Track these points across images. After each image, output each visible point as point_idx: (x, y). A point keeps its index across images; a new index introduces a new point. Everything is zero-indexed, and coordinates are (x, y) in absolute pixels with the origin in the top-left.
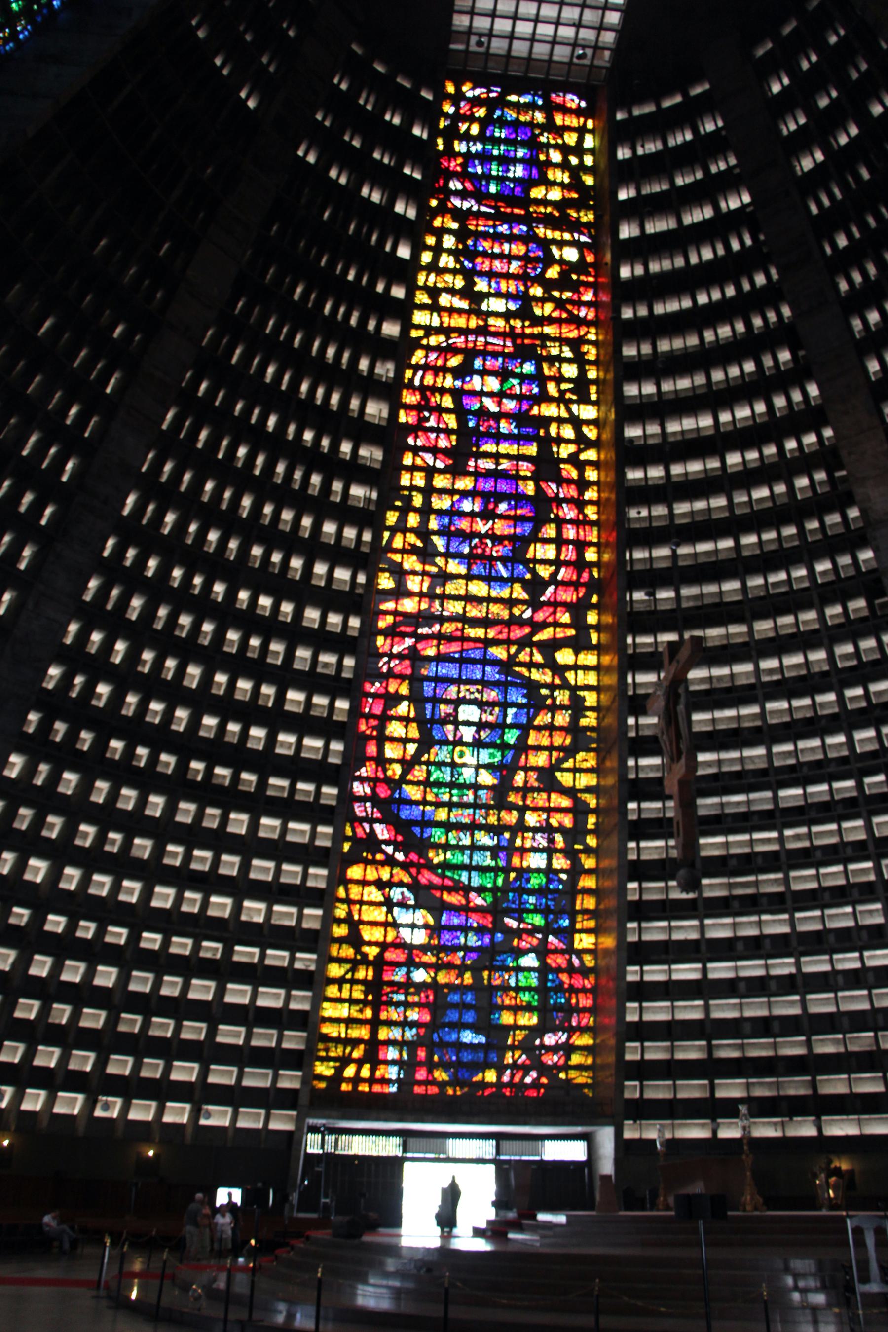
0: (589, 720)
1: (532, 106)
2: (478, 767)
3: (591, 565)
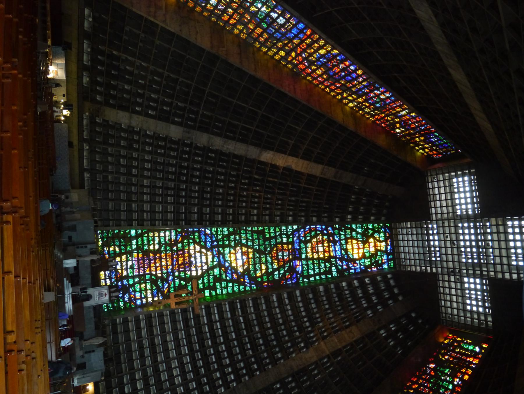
0: (257, 45)
1: (446, 152)
2: (259, 10)
3: (307, 76)
